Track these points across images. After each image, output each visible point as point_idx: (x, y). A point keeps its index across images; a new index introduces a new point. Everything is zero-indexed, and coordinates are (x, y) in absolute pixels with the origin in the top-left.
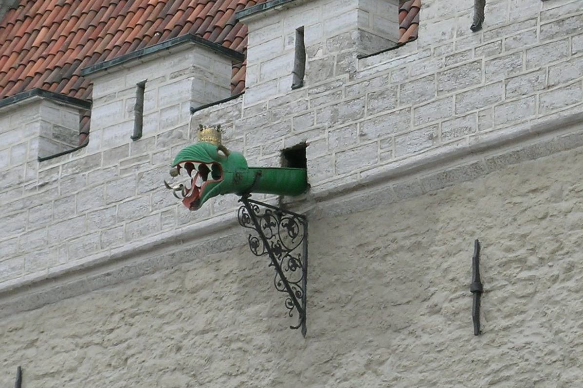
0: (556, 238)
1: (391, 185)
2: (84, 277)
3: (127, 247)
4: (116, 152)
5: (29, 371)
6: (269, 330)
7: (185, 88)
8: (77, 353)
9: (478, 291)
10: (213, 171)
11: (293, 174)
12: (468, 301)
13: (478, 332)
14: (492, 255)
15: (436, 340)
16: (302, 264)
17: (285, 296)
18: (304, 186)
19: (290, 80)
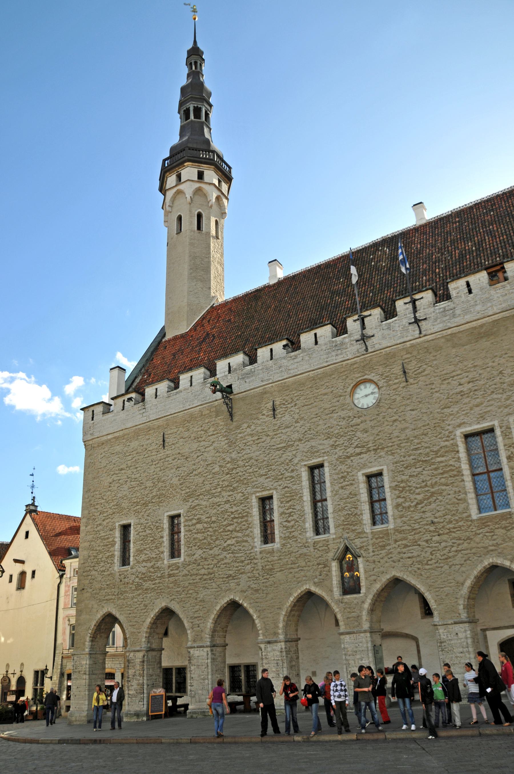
0: (292, 399)
1: (252, 391)
2: (178, 414)
3: (189, 407)
4: (185, 389)
5: (166, 433)
6: (223, 421)
7: (202, 376)
8: (177, 429)
9: (274, 410)
11: (229, 390)
12: (272, 413)
13: (275, 418)
14: (277, 403)
15: (264, 420)
16: (231, 408)
17: (229, 413)
18: (232, 392)
19: (227, 372)
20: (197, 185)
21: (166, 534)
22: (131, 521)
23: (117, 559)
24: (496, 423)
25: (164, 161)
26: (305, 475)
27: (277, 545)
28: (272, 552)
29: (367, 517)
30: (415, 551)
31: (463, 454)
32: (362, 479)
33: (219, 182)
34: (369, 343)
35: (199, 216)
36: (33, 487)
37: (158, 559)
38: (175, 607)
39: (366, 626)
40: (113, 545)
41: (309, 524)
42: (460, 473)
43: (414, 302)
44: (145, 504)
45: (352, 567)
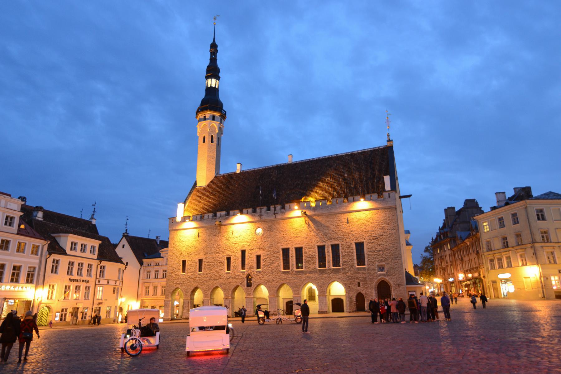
21: (198, 264)
24: (290, 247)
28: (229, 273)
29: (255, 267)
30: (266, 277)
32: (255, 256)
34: (262, 217)
36: (126, 225)
40: (179, 266)
43: (275, 208)
44: (191, 254)
45: (250, 280)
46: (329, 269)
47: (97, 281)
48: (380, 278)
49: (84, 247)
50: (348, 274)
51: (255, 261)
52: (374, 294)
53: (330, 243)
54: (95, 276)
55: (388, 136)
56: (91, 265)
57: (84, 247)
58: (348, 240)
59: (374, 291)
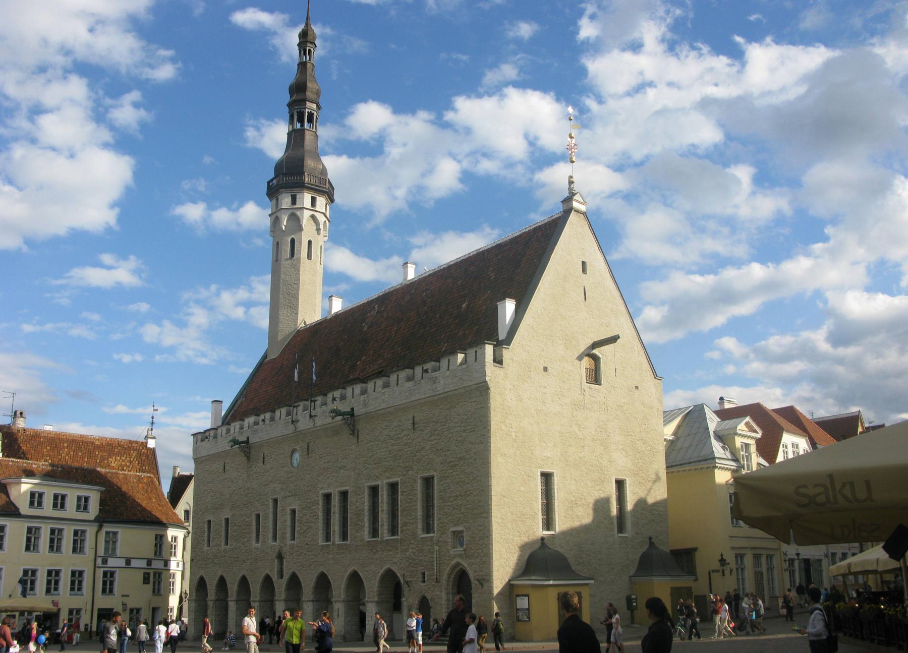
10: (235, 442)
16: (249, 453)
20: (290, 211)
21: (224, 529)
22: (212, 519)
23: (206, 543)
25: (269, 183)
26: (271, 504)
27: (259, 545)
29: (289, 535)
31: (321, 507)
32: (289, 512)
33: (313, 200)
35: (293, 241)
37: (220, 546)
38: (225, 575)
39: (283, 597)
41: (270, 535)
42: (318, 519)
46: (382, 542)
47: (99, 561)
48: (453, 562)
49: (59, 502)
50: (407, 554)
51: (289, 523)
52: (444, 602)
53: (385, 482)
54: (94, 551)
55: (571, 183)
56: (83, 532)
57: (59, 502)
58: (410, 472)
59: (444, 596)
